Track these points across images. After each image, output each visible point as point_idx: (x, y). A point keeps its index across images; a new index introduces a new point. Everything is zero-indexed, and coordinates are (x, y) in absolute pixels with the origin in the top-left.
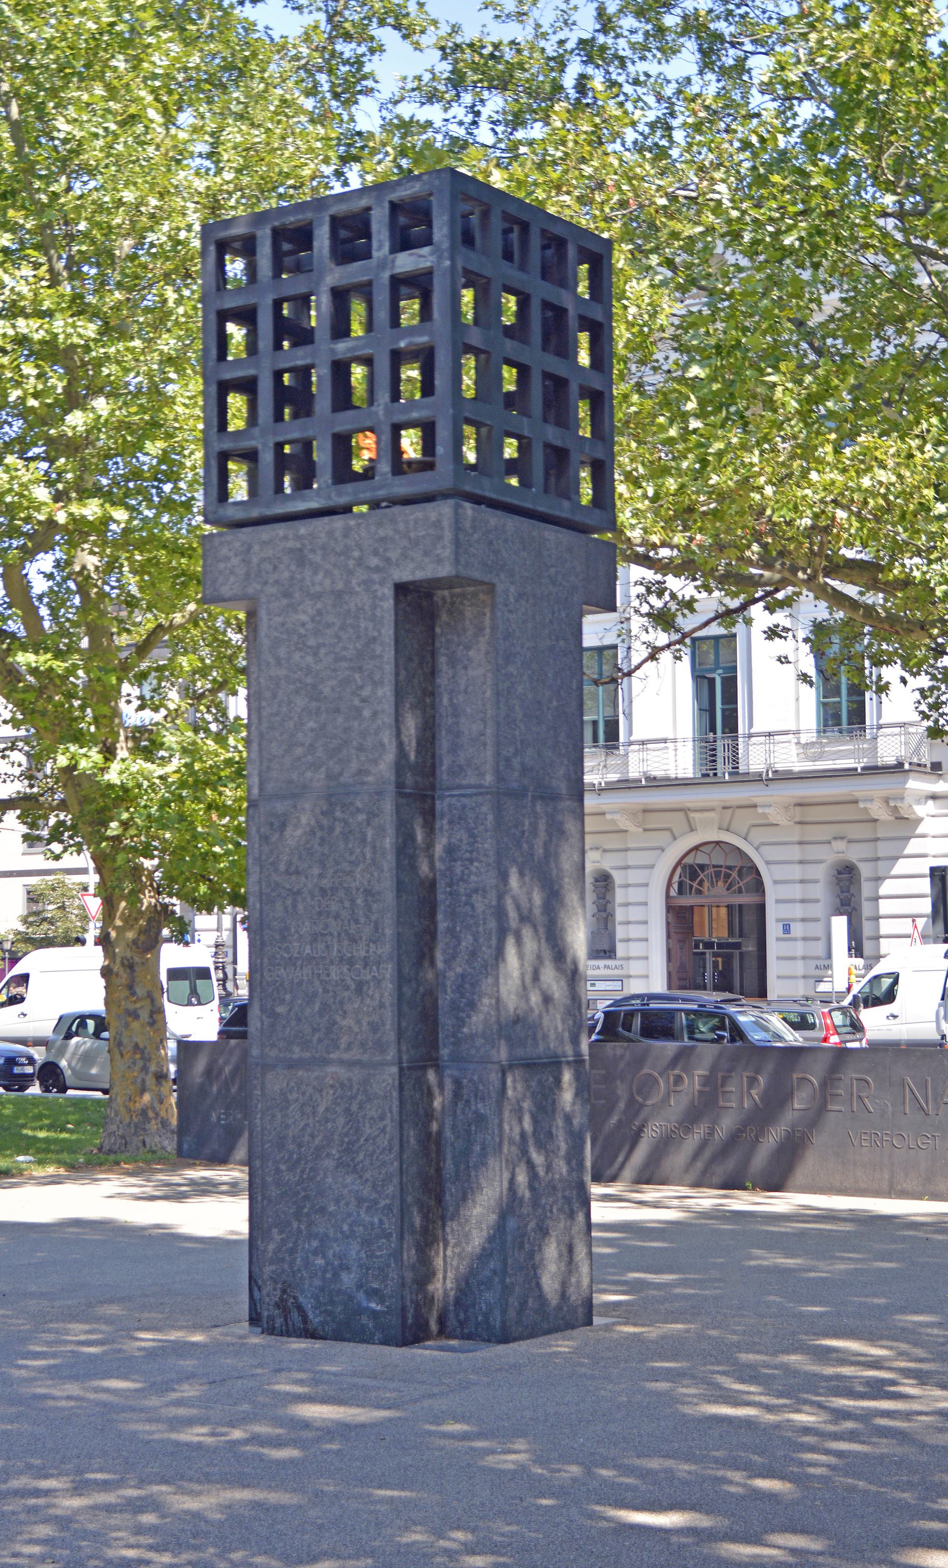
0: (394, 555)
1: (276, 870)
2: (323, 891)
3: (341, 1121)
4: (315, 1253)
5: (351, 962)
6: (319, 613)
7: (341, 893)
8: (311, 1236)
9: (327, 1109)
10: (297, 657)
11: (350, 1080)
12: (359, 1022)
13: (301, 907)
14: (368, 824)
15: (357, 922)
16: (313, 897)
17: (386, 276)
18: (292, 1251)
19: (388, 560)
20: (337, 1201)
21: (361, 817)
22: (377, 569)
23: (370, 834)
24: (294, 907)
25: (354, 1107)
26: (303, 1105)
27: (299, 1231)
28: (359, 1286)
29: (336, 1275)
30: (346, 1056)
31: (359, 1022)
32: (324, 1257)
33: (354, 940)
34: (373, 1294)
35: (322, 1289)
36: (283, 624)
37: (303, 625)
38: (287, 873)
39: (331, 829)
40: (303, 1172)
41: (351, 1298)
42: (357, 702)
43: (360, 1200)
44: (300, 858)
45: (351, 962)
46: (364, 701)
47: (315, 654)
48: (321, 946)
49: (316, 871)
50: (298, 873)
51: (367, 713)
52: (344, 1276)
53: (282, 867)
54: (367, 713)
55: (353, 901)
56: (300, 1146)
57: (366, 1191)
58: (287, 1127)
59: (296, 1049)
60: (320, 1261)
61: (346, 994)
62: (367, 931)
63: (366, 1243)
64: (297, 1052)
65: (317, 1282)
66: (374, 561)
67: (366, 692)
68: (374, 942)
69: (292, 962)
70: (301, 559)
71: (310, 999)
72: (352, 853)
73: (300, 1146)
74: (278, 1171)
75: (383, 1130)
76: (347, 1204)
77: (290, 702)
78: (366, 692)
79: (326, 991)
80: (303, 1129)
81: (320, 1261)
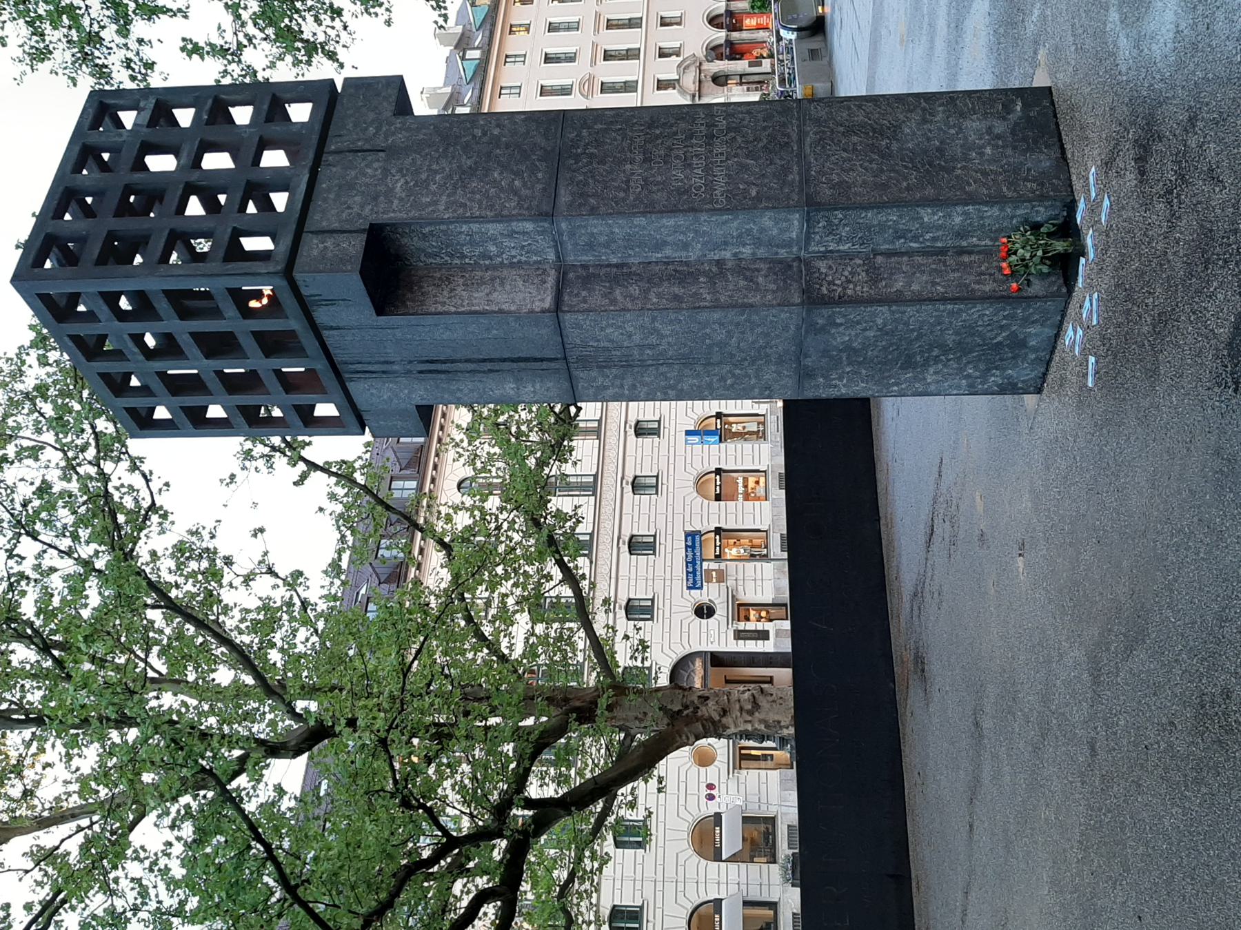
0: (371, 116)
1: (624, 200)
2: (645, 160)
3: (855, 139)
4: (982, 154)
6: (400, 170)
7: (649, 146)
8: (966, 158)
9: (845, 150)
10: (433, 187)
11: (816, 133)
12: (764, 129)
13: (659, 179)
14: (592, 127)
15: (676, 133)
16: (652, 169)
17: (145, 130)
18: (985, 174)
19: (373, 121)
20: (929, 139)
21: (585, 132)
22: (378, 129)
23: (599, 126)
24: (658, 183)
25: (842, 129)
26: (842, 169)
27: (963, 168)
28: (1004, 119)
29: (998, 137)
30: (794, 136)
31: (764, 129)
32: (983, 147)
33: (691, 136)
35: (1015, 148)
36: (401, 199)
37: (407, 183)
38: (626, 191)
39: (591, 156)
40: (906, 167)
41: (1016, 124)
42: (485, 139)
43: (925, 121)
44: (613, 180)
46: (485, 134)
47: (436, 172)
48: (695, 161)
49: (628, 167)
50: (628, 181)
51: (496, 132)
52: (997, 131)
53: (622, 194)
54: (496, 132)
55: (657, 137)
56: (882, 171)
57: (916, 117)
58: (864, 182)
59: (790, 177)
60: (988, 150)
61: (739, 139)
62: (683, 125)
63: (962, 115)
64: (794, 177)
65: (1009, 151)
67: (478, 132)
68: (695, 119)
69: (710, 186)
70: (351, 186)
71: (744, 168)
72: (615, 139)
73: (882, 171)
74: (908, 189)
75: (860, 107)
76: (930, 131)
77: (473, 192)
78: (478, 132)
79: (736, 155)
80: (866, 169)
81: (988, 150)
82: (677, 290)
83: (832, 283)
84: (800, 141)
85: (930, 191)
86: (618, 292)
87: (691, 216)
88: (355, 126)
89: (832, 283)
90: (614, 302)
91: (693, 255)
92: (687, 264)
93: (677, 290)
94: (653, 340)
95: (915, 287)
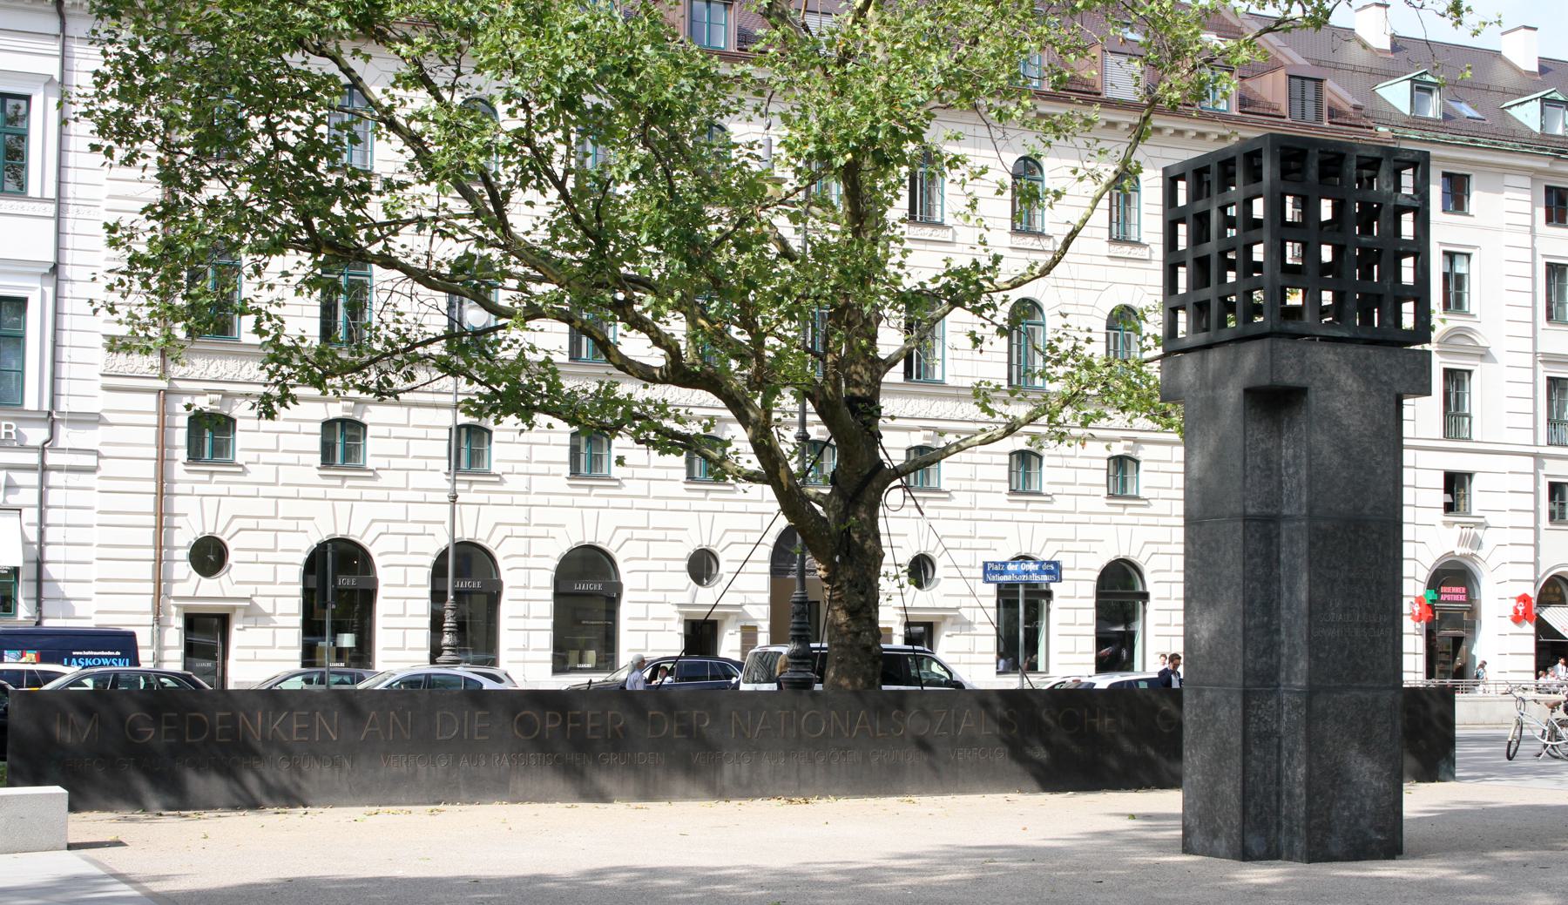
0: (1396, 376)
2: (1351, 581)
4: (1344, 809)
5: (1368, 626)
18: (1329, 809)
21: (1375, 536)
22: (1385, 383)
29: (1357, 821)
34: (1380, 830)
43: (1372, 773)
45: (1368, 626)
50: (1335, 568)
60: (1346, 813)
66: (1385, 378)
81: (1346, 813)
82: (1258, 602)
83: (1259, 707)
84: (1360, 688)
85: (1317, 772)
86: (1257, 560)
87: (1306, 612)
88: (1390, 366)
89: (1259, 707)
90: (1251, 557)
91: (1283, 612)
92: (1278, 608)
93: (1258, 602)
94: (1225, 583)
95: (1254, 763)
